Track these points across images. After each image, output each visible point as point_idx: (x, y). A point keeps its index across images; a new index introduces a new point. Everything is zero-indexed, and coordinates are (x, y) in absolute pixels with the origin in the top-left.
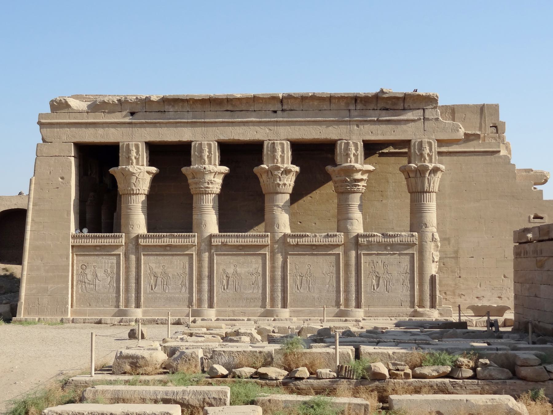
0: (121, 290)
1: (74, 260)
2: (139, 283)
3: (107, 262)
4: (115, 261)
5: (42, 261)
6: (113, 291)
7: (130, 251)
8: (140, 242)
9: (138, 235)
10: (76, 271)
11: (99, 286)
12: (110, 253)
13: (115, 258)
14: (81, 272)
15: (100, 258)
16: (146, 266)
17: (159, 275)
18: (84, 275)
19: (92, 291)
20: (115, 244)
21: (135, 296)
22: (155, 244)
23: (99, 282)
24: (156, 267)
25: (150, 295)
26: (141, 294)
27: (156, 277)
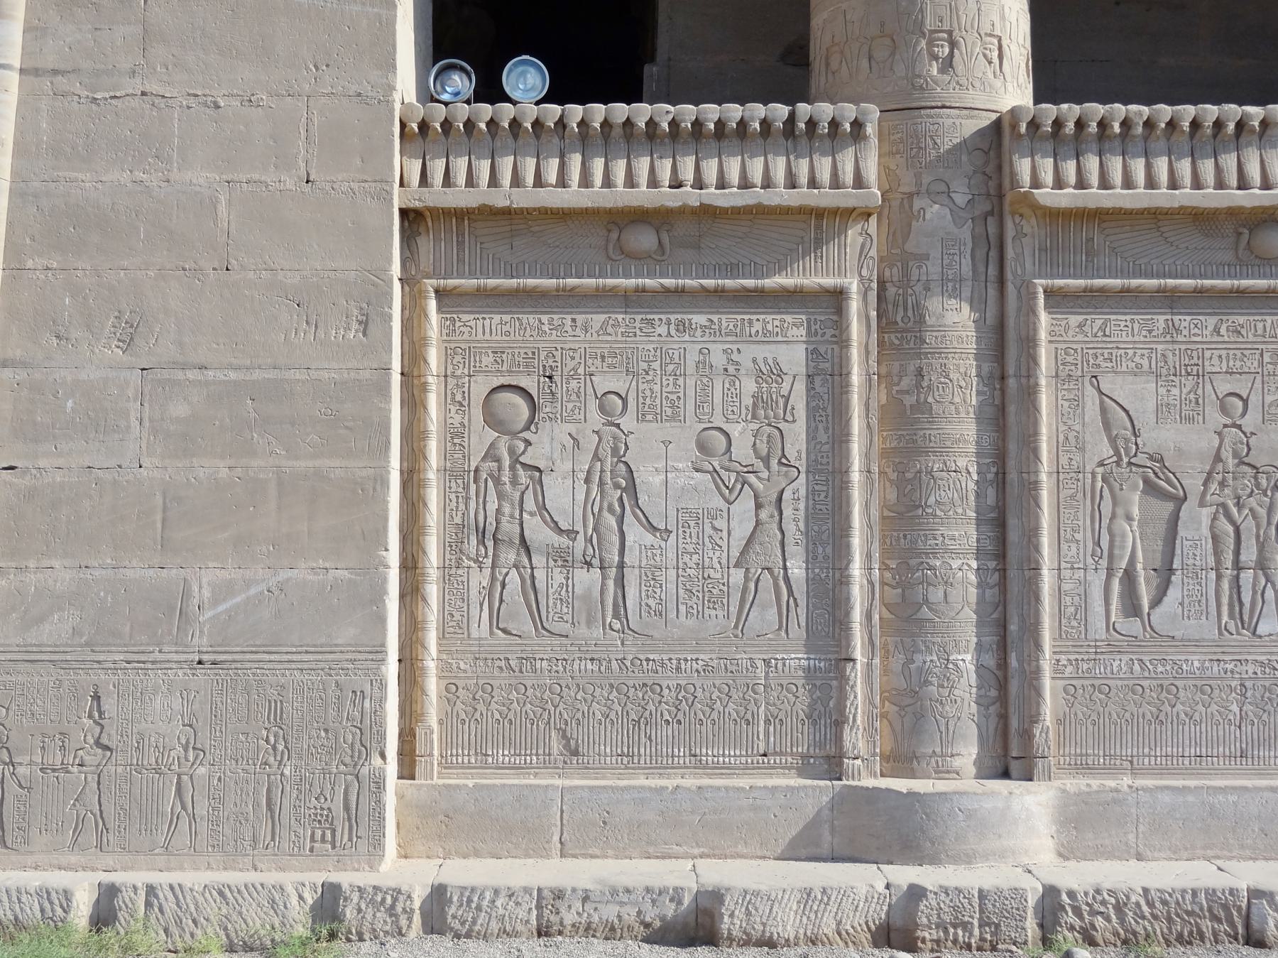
0: (857, 615)
1: (424, 342)
2: (1013, 554)
3: (718, 359)
4: (794, 358)
5: (128, 344)
6: (783, 626)
7: (933, 269)
8: (1026, 178)
9: (997, 125)
10: (443, 442)
11: (651, 575)
12: (750, 283)
13: (794, 326)
14: (491, 454)
15: (663, 324)
16: (1077, 403)
17: (1194, 484)
18: (514, 481)
19: (589, 623)
20: (802, 196)
21: (980, 668)
22: (1163, 197)
23: (649, 539)
24: (1162, 410)
25: (1119, 663)
26: (1038, 646)
27: (1165, 496)
